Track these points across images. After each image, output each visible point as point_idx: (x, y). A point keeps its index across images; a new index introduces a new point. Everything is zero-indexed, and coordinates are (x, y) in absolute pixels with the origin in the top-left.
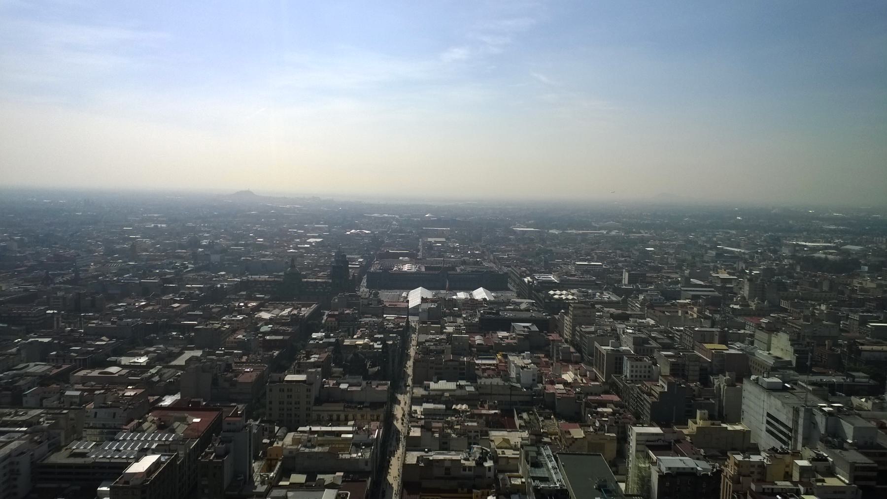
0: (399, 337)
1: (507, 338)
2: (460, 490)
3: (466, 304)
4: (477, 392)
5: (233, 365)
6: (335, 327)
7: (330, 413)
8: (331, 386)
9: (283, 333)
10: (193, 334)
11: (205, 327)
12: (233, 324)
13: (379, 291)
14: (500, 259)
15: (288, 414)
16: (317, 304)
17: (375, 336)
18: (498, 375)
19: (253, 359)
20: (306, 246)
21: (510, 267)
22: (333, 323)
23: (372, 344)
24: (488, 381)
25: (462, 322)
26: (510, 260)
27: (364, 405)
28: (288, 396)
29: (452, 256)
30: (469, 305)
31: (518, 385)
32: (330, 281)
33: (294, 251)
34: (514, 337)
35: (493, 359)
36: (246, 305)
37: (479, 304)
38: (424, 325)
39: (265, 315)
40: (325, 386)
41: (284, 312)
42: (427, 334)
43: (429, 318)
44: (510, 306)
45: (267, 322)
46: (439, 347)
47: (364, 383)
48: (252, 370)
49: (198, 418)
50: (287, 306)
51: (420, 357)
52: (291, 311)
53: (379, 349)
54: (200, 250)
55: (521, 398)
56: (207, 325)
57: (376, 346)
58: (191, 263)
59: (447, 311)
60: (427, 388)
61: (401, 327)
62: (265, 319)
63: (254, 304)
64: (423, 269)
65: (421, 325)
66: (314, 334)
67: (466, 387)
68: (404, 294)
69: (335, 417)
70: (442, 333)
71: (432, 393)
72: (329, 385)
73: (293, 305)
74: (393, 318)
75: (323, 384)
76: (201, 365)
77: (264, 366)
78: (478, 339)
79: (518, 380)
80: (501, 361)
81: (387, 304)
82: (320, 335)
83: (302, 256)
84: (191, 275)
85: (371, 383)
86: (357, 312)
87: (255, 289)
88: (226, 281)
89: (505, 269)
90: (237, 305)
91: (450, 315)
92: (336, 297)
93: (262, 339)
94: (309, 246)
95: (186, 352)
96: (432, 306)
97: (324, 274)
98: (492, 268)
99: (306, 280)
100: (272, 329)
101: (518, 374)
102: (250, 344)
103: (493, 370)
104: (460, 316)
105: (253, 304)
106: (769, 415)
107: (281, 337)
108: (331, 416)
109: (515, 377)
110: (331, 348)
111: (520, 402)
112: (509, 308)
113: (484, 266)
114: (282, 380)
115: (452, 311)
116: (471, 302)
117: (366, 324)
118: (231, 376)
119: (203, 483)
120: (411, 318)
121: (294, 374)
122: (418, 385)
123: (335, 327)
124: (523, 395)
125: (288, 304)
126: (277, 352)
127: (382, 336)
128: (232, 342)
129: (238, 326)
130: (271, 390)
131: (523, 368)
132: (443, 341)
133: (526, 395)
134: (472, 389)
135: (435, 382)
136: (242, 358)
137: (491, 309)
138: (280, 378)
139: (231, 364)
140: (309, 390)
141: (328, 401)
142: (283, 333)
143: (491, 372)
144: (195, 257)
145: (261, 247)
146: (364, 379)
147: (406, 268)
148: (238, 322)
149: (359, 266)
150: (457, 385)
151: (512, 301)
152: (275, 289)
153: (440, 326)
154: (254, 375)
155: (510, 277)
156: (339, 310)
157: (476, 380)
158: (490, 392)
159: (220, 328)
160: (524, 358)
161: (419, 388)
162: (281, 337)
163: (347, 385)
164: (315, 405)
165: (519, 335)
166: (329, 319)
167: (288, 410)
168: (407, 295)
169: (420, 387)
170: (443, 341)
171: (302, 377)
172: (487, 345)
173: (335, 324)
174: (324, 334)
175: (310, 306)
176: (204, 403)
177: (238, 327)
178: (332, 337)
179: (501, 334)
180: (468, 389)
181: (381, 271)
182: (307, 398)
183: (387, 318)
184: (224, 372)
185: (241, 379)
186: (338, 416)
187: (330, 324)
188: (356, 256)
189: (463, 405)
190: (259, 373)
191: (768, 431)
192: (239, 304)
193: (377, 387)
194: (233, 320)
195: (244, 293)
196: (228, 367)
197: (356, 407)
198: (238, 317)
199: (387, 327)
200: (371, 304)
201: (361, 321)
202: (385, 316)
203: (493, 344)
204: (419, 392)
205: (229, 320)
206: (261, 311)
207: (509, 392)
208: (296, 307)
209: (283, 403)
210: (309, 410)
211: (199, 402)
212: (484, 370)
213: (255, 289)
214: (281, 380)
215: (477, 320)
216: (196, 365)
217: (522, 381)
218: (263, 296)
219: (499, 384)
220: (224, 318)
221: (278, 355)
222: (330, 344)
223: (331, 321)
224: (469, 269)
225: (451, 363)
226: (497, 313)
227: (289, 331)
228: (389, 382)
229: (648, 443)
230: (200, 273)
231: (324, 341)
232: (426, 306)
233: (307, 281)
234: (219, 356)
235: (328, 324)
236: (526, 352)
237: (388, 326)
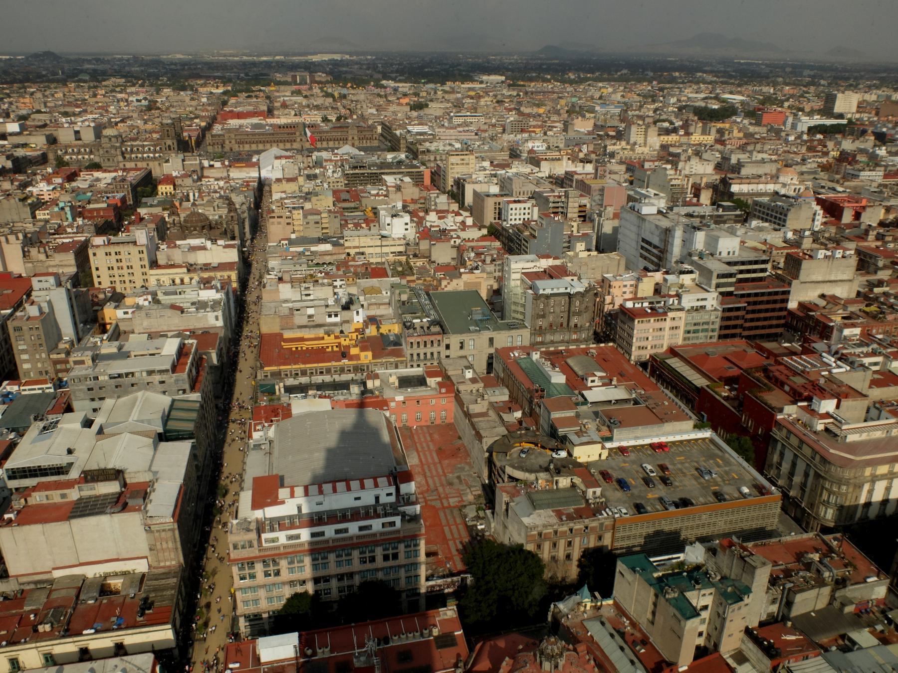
2: (326, 337)
7: (172, 277)
55: (394, 249)
69: (178, 281)
106: (643, 240)
119: (20, 348)
146: (209, 239)
186: (182, 280)
191: (642, 256)
229: (524, 271)
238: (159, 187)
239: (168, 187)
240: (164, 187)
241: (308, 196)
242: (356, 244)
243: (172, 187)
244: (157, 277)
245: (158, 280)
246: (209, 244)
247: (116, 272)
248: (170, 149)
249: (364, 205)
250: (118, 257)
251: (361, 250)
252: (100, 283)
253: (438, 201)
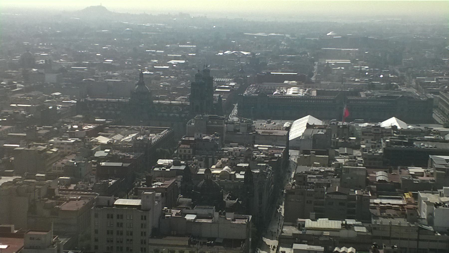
0: (270, 168)
1: (422, 174)
3: (368, 132)
4: (370, 234)
5: (56, 191)
6: (189, 156)
8: (174, 215)
9: (124, 160)
10: (13, 158)
11: (27, 149)
12: (63, 148)
13: (254, 122)
14: (423, 84)
15: (118, 247)
16: (169, 129)
17: (238, 165)
18: (404, 215)
19: (83, 186)
20: (164, 67)
21: (438, 93)
22: (187, 150)
23: (233, 173)
24: (386, 221)
25: (360, 154)
26: (439, 85)
27: (216, 241)
28: (118, 224)
29: (357, 80)
30: (371, 134)
31: (431, 228)
32: (188, 103)
33: (149, 73)
34: (432, 174)
35: (400, 199)
36: (80, 128)
37: (385, 132)
38: (305, 155)
39: (103, 140)
40: (166, 216)
41: (127, 138)
42: (309, 165)
43: (314, 147)
44: (431, 136)
45: (103, 147)
46: (323, 180)
47: (216, 215)
48: (79, 197)
49: (4, 244)
50: (131, 131)
51: (294, 187)
52: (136, 137)
53: (241, 179)
54: (34, 70)
56: (29, 147)
57: (238, 176)
58: (20, 83)
59: (340, 141)
60: (301, 226)
61: (276, 158)
62: (103, 144)
63: (91, 127)
64: (314, 93)
65: (302, 155)
66: (159, 160)
67: (355, 227)
68: (286, 124)
70: (330, 166)
71: (308, 232)
72: (171, 215)
73: (139, 130)
74: (267, 149)
75: (163, 213)
76: (16, 187)
77: (96, 195)
78: (380, 175)
79: (430, 222)
80: (409, 203)
81: (260, 132)
82: (167, 161)
83: (158, 78)
84: (19, 96)
85: (224, 214)
86: (218, 138)
87: (95, 111)
88: (61, 103)
89: (431, 96)
90: (69, 127)
91: (344, 145)
92: (192, 120)
93: (96, 166)
94: (168, 67)
95: (3, 177)
96: (320, 133)
97: (183, 99)
98: (410, 93)
99: (157, 101)
100: (109, 154)
101: (430, 214)
102: (81, 169)
103: (396, 209)
104: (358, 147)
105: (89, 127)
107: (120, 164)
109: (426, 218)
110: (180, 177)
112: (428, 139)
113: (400, 90)
114: (111, 204)
115: (347, 141)
116: (375, 130)
117: (230, 153)
118: (52, 203)
120: (291, 152)
121: (128, 199)
122: (291, 223)
124: (436, 241)
125: (133, 129)
126: (113, 181)
127: (247, 165)
128: (59, 168)
129: (69, 151)
130: (96, 216)
131: (437, 205)
132: (330, 174)
133: (441, 241)
134: (364, 230)
135: (312, 220)
136: (69, 185)
137: (403, 138)
138: (109, 202)
139: (54, 190)
141: (169, 235)
142: (124, 160)
143: (391, 212)
144: (26, 77)
145: (109, 67)
147: (290, 92)
148: (70, 146)
149: (229, 90)
150: (342, 225)
151: (434, 130)
152: (118, 113)
153: (328, 156)
154: (81, 204)
155: (436, 107)
156: (195, 135)
157: (371, 220)
158: (389, 236)
159: (45, 150)
160: (441, 195)
161: (291, 227)
162: (120, 164)
163: (195, 216)
164: (152, 237)
165: (437, 169)
166: (182, 146)
167: (118, 242)
168: (291, 125)
169: (293, 225)
170: (330, 174)
171: (137, 202)
172: (392, 182)
173: (189, 152)
174: (172, 161)
175: (159, 131)
176: (16, 231)
177: (69, 153)
178: (183, 165)
179: (413, 170)
180: (357, 229)
181: (257, 95)
182: (142, 227)
183: (259, 148)
184: (43, 197)
185: (65, 207)
187: (183, 152)
188: (227, 80)
189: (348, 247)
190: (87, 201)
192: (72, 127)
193: (234, 220)
194: (62, 144)
195: (80, 116)
196: (50, 193)
197: (205, 243)
198: (70, 139)
199: (256, 157)
200: (239, 131)
201: (223, 150)
202: (256, 146)
203: (401, 182)
204: (289, 230)
205: (58, 144)
206: (100, 135)
207: (415, 236)
208: (142, 132)
209: (112, 233)
210: (145, 243)
211: (10, 229)
212: (384, 209)
213: (95, 111)
214: (111, 205)
215: (381, 151)
216: (9, 187)
217: (436, 222)
218: (104, 120)
219: (402, 225)
220: (52, 140)
221: (114, 184)
222: (178, 172)
223: (184, 148)
224: (378, 93)
225: (335, 197)
226: (410, 143)
227: (131, 158)
228: (250, 217)
230: (30, 94)
231: (172, 168)
232: (311, 132)
233: (159, 103)
234: (40, 180)
235: (181, 151)
236: (444, 188)
237: (258, 156)
244: (156, 247)
250: (120, 221)
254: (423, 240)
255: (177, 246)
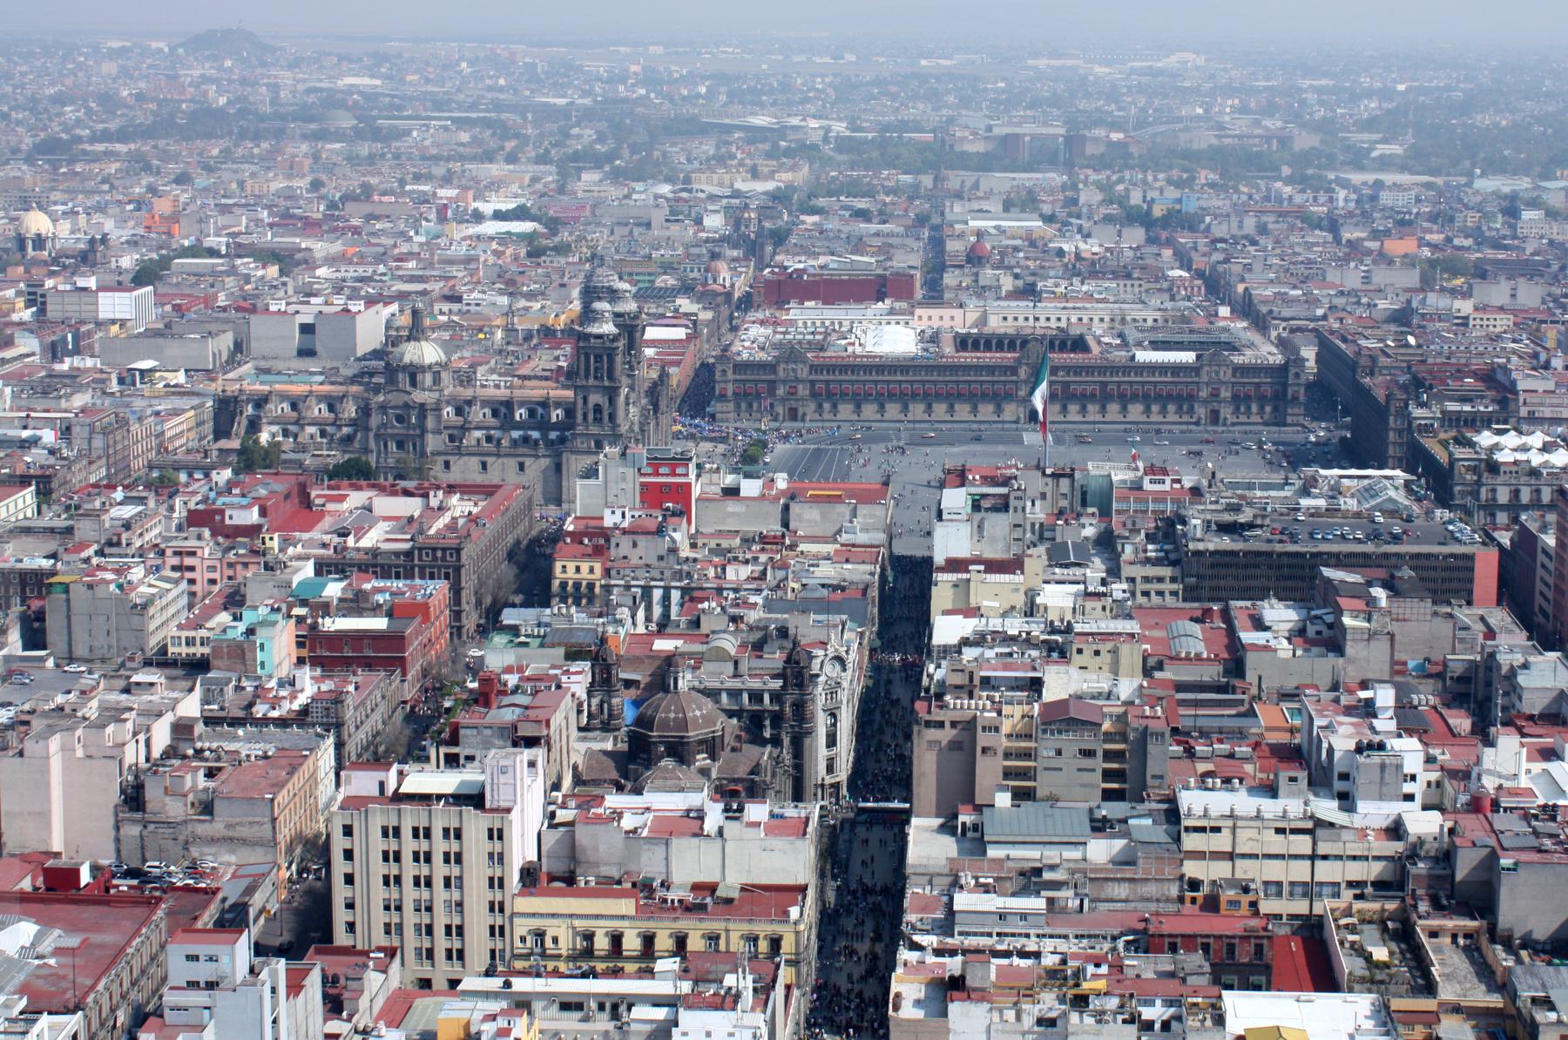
7: (580, 924)
55: (1356, 871)
69: (602, 943)
107: (380, 623)
108: (589, 937)
111: (1350, 884)
123: (591, 586)
130: (348, 831)
140: (496, 834)
186: (616, 940)
238: (558, 566)
239: (585, 567)
240: (571, 566)
241: (1059, 645)
242: (1221, 842)
243: (598, 567)
245: (540, 934)
246: (714, 816)
247: (410, 894)
248: (598, 420)
249: (1251, 676)
251: (1245, 869)
252: (351, 926)
253: (1522, 679)
254: (1325, 857)
255: (597, 917)
